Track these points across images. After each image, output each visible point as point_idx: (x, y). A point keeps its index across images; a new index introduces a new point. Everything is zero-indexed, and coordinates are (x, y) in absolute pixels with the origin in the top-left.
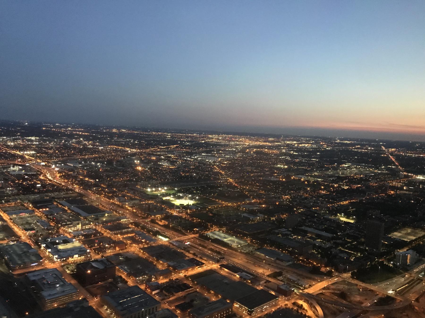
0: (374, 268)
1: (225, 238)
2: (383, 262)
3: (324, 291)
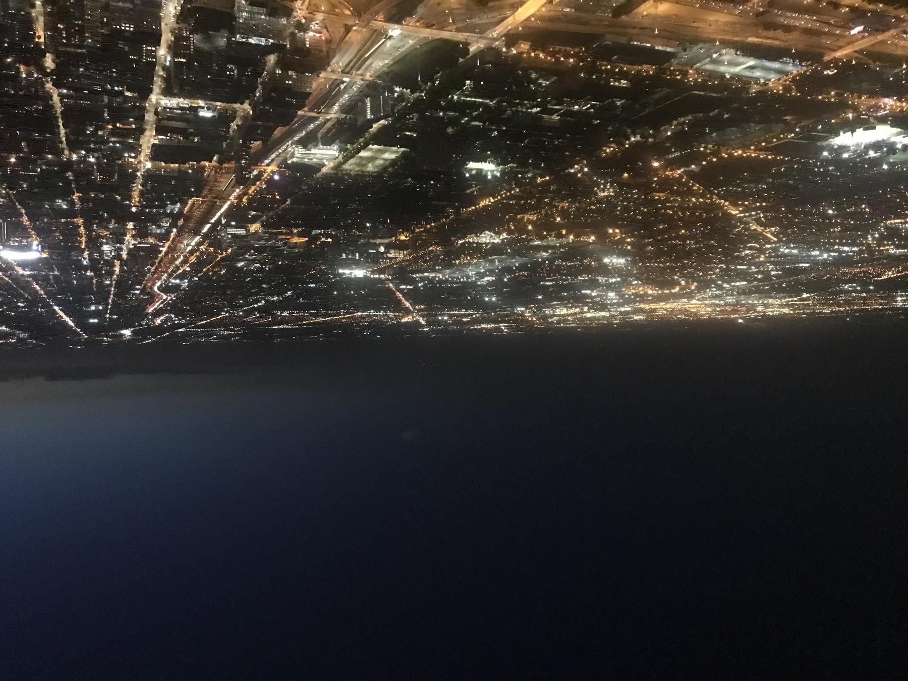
1: (752, 68)
2: (412, 92)
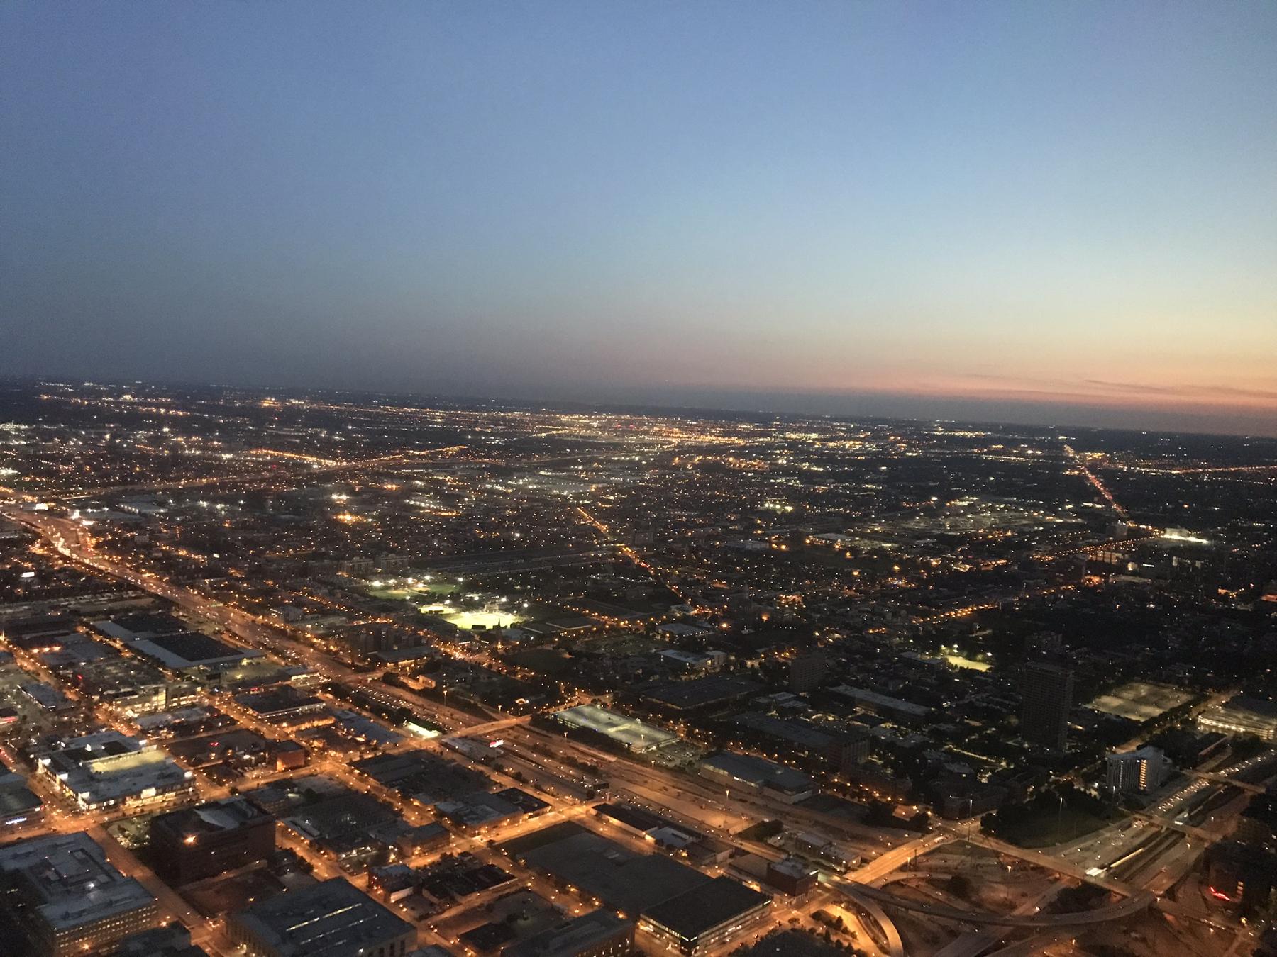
0: (1045, 802)
1: (612, 725)
2: (1070, 784)
3: (902, 876)
